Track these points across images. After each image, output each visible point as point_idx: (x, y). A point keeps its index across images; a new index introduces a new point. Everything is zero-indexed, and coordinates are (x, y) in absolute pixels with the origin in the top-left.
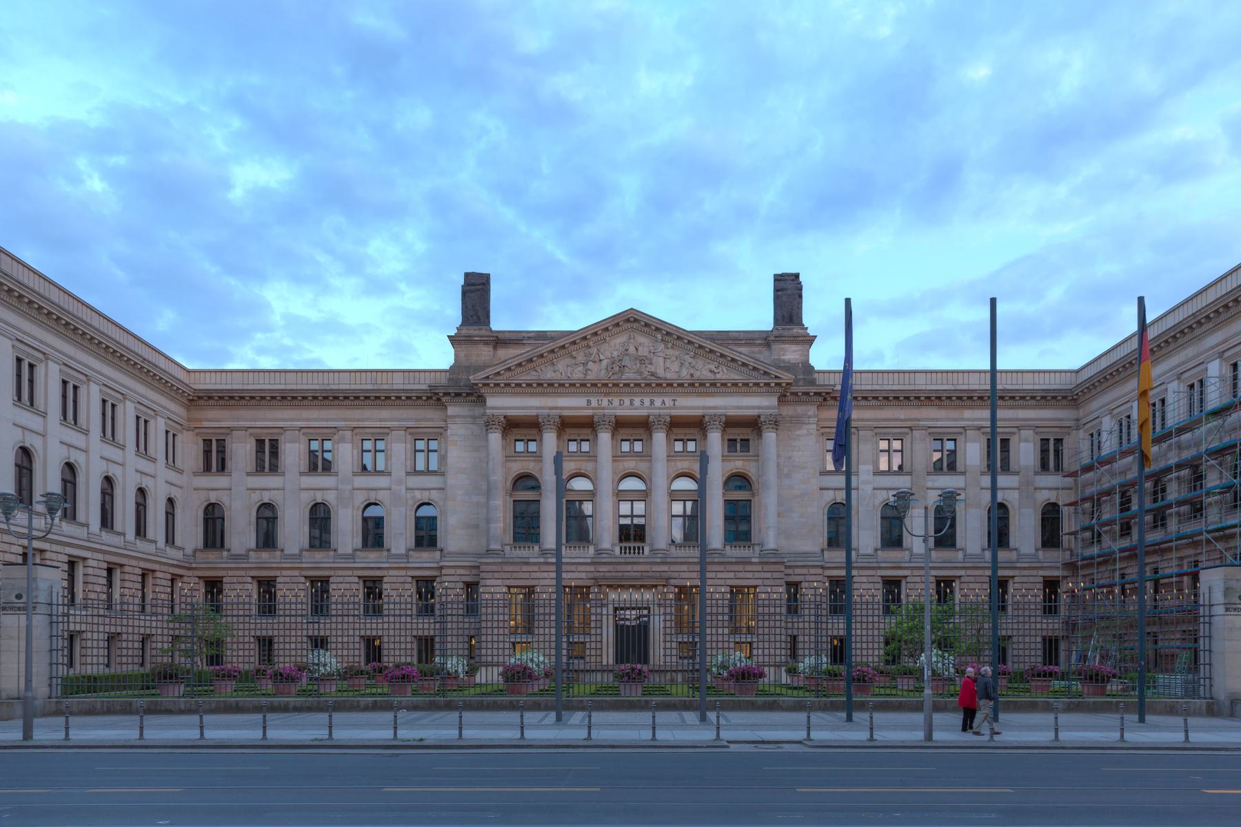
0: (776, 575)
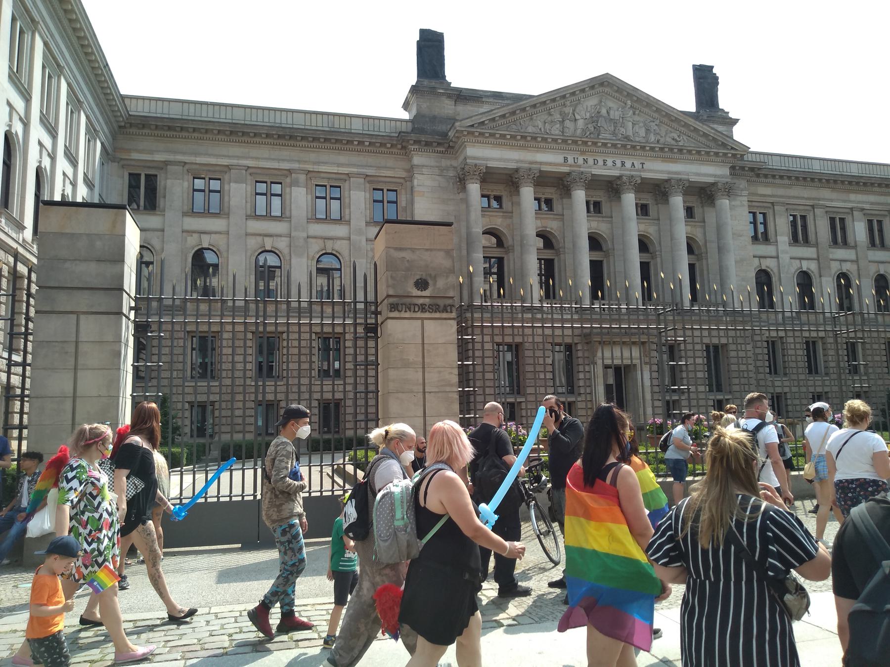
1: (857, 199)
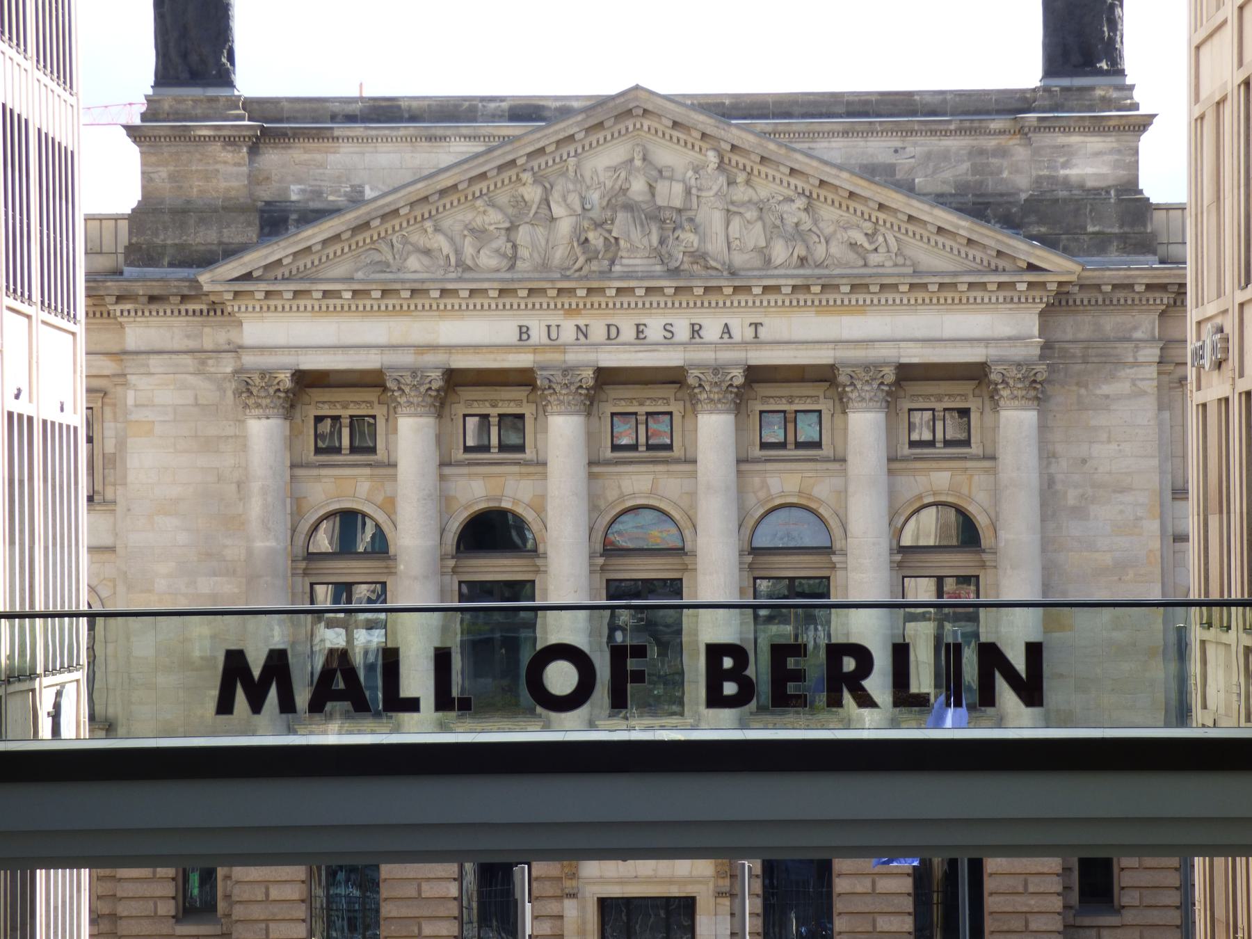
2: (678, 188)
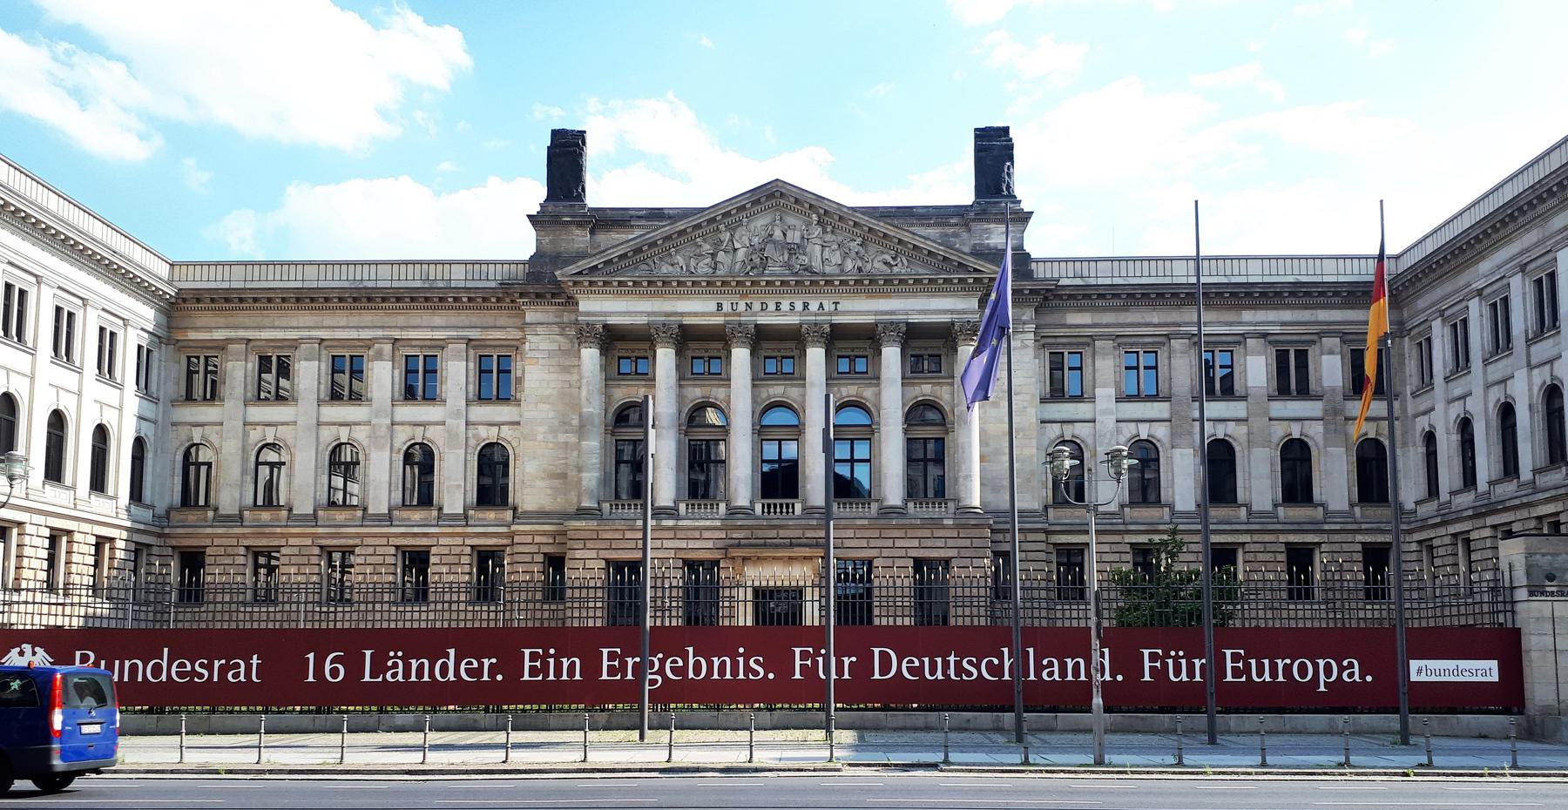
0: (976, 543)
1: (1252, 318)
2: (798, 234)
